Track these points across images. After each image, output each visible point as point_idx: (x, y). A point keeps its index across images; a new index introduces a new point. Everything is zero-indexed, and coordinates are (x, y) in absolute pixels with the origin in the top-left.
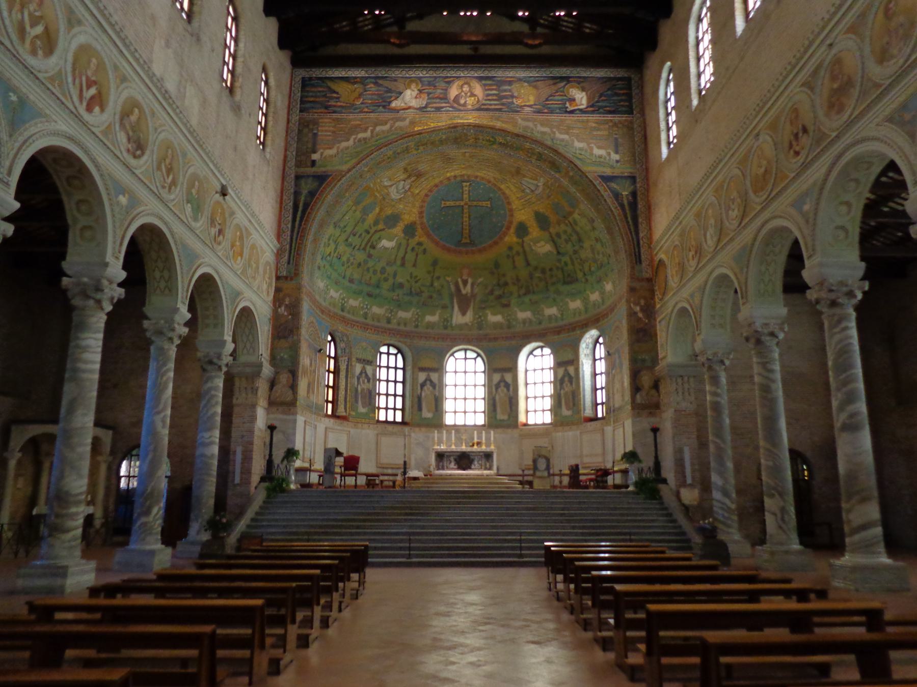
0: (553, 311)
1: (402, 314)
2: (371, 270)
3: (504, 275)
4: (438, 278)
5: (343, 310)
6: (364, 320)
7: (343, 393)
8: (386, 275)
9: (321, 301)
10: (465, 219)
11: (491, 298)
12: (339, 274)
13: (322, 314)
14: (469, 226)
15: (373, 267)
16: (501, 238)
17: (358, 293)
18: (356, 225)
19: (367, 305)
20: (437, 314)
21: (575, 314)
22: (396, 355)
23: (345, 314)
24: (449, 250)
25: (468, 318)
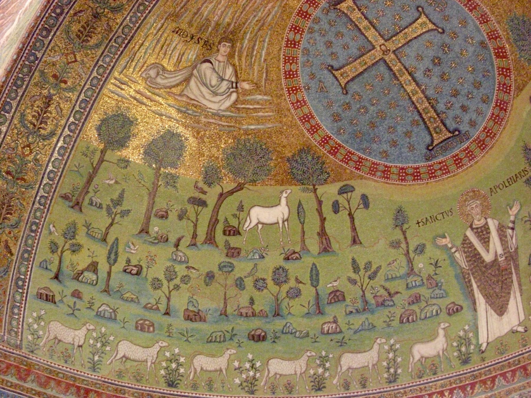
2: (249, 282)
4: (421, 249)
5: (171, 384)
8: (292, 283)
10: (409, 89)
12: (145, 307)
14: (428, 99)
15: (249, 275)
18: (153, 194)
20: (441, 332)
24: (416, 176)
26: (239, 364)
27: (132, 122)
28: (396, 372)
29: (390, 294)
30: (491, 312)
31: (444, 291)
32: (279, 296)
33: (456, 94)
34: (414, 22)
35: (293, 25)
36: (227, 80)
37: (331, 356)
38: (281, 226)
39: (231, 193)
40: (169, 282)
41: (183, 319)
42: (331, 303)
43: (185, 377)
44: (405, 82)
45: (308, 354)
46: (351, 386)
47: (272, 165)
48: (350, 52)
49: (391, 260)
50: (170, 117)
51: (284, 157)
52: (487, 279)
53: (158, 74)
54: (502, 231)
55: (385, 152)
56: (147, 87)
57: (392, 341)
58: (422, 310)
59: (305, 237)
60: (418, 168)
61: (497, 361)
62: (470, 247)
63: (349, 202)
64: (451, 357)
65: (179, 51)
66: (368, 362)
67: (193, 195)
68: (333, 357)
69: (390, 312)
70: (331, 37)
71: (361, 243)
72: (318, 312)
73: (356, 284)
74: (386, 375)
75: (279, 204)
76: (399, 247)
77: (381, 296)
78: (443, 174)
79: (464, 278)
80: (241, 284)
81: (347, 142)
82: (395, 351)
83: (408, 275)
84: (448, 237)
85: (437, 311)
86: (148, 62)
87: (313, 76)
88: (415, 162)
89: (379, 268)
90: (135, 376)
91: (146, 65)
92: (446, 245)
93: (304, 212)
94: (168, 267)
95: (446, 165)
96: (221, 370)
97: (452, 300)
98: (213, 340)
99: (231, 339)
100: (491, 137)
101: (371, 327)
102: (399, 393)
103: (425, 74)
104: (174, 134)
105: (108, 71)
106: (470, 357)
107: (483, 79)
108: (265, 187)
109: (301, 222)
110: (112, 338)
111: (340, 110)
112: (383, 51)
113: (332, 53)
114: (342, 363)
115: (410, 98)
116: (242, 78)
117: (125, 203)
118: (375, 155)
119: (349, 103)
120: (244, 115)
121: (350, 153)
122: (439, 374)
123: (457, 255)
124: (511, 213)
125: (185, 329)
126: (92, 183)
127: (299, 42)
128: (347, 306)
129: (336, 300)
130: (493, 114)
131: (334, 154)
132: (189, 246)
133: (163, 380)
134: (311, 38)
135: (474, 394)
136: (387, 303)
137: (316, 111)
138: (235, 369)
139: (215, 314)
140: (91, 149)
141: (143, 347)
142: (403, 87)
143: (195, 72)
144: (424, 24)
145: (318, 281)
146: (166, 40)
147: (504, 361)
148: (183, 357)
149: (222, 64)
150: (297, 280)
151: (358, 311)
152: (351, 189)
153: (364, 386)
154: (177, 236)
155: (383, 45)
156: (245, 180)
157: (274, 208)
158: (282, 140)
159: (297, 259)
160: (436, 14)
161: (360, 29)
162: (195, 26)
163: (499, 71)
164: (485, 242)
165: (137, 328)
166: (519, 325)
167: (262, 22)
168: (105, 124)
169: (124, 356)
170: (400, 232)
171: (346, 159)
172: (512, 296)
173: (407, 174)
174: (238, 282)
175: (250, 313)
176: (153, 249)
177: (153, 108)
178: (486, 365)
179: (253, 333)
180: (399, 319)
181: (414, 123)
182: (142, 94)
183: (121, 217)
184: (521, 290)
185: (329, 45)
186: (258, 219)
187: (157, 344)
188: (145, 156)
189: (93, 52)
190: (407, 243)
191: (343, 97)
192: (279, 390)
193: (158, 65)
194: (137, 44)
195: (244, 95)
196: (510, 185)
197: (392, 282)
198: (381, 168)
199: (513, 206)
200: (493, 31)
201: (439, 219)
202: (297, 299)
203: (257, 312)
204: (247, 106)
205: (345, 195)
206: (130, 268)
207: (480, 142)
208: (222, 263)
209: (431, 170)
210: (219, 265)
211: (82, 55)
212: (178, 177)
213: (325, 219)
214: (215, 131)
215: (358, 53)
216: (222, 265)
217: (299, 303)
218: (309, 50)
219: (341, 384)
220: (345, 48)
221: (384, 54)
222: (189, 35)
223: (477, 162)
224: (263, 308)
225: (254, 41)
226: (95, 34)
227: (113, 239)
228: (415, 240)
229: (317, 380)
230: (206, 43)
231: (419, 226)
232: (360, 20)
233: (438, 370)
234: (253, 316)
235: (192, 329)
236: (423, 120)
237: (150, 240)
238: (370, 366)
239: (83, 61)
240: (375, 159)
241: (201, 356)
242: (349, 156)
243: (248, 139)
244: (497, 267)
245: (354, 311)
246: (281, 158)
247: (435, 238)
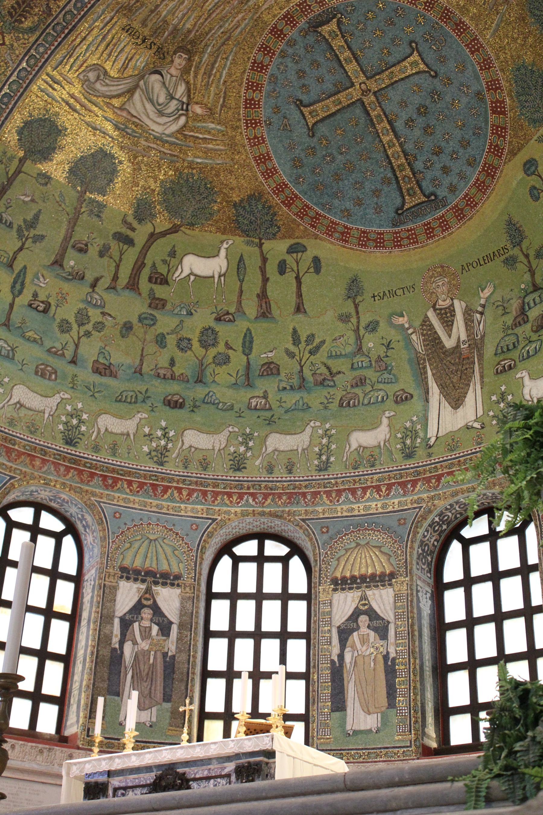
2: (171, 340)
4: (373, 327)
5: (69, 442)
7: (80, 669)
8: (221, 348)
10: (385, 139)
11: (526, 330)
12: (49, 351)
14: (406, 154)
15: (173, 332)
16: (497, 151)
18: (73, 222)
20: (385, 421)
22: (284, 560)
23: (80, 451)
26: (150, 430)
27: (60, 131)
28: (328, 459)
29: (331, 374)
31: (394, 375)
33: (438, 151)
34: (404, 60)
35: (263, 44)
36: (178, 100)
37: (256, 434)
38: (216, 280)
39: (164, 234)
40: (79, 327)
41: (90, 370)
42: (262, 375)
43: (87, 436)
44: (382, 131)
45: (230, 429)
46: (276, 470)
47: (215, 208)
48: (324, 87)
49: (337, 335)
50: (104, 133)
51: (230, 201)
52: (445, 367)
53: (98, 78)
54: (469, 315)
55: (348, 210)
56: (83, 91)
57: (328, 426)
58: (365, 395)
60: (383, 234)
61: (445, 458)
62: (429, 330)
63: (298, 263)
64: (393, 449)
65: (126, 55)
66: (298, 446)
67: (119, 230)
68: (259, 435)
69: (329, 393)
70: (305, 65)
71: (306, 312)
72: (246, 383)
73: (294, 357)
74: (316, 462)
75: (218, 255)
77: (321, 374)
78: (410, 243)
80: (162, 340)
81: (306, 194)
82: (329, 437)
83: (354, 354)
84: (406, 316)
85: (383, 398)
86: (89, 62)
87: (277, 109)
88: (380, 226)
89: (323, 342)
90: (28, 427)
91: (85, 65)
92: (403, 325)
93: (245, 269)
94: (80, 309)
95: (415, 234)
96: (128, 435)
97: (402, 388)
98: (123, 399)
99: (144, 401)
100: (471, 207)
101: (305, 407)
102: (329, 483)
103: (406, 124)
104: (106, 154)
105: (40, 64)
106: (415, 451)
107: (473, 137)
108: (204, 233)
109: (239, 280)
110: (6, 380)
111: (302, 155)
112: (362, 90)
113: (304, 85)
114: (267, 443)
115: (385, 151)
116: (194, 100)
117: (39, 226)
118: (335, 213)
119: (314, 147)
120: (192, 144)
121: (307, 206)
122: (378, 467)
123: (414, 337)
124: (482, 295)
125: (92, 383)
126: (5, 196)
127: (267, 66)
128: (281, 381)
129: (269, 373)
130: (478, 180)
131: (289, 206)
132: (107, 288)
133: (61, 435)
134: (282, 63)
135: (416, 491)
137: (275, 152)
138: (145, 436)
139: (128, 371)
140: (9, 155)
141: (42, 395)
142: (379, 136)
143: (142, 83)
144: (414, 64)
145: (251, 349)
146: (113, 38)
147: (454, 459)
148: (86, 413)
149: (174, 78)
150: (227, 344)
152: (302, 250)
153: (290, 472)
154: (96, 275)
155: (364, 83)
156: (182, 221)
157: (211, 259)
158: (231, 181)
159: (230, 321)
160: (431, 53)
161: (340, 61)
162: (149, 27)
163: (492, 130)
164: (447, 326)
165: (36, 373)
166: (475, 421)
167: (228, 35)
168: (28, 128)
169: (18, 402)
171: (302, 213)
173: (369, 240)
174: (159, 339)
175: (169, 375)
176: (66, 287)
177: (87, 119)
178: (433, 461)
179: (169, 398)
180: (338, 402)
181: (386, 181)
182: (76, 100)
183: (33, 242)
184: (482, 382)
185: (301, 74)
186: (191, 269)
187: (58, 395)
188: (70, 175)
189: (26, 37)
190: (358, 318)
191: (308, 139)
192: (192, 464)
193: (100, 68)
194: (79, 36)
195: (194, 120)
196: (485, 263)
197: (336, 361)
198: (340, 229)
199: (486, 287)
200: (495, 81)
201: (398, 294)
202: (224, 366)
203: (177, 374)
204: (197, 135)
205: (294, 255)
206: (37, 303)
207: (457, 211)
208: (143, 313)
209: (397, 238)
210: (140, 316)
211: (12, 38)
212: (105, 206)
213: (268, 279)
214: (155, 158)
215: (334, 89)
216: (143, 316)
217: (226, 372)
218: (277, 78)
219: (264, 467)
220: (319, 81)
221: (362, 94)
222: (141, 37)
223: (451, 234)
224: (184, 371)
225: (215, 55)
226: (31, 14)
227: (21, 266)
228: (368, 316)
229: (237, 459)
230: (159, 50)
231: (375, 300)
232: (342, 50)
233: (377, 462)
234: (172, 379)
235: (101, 384)
236: (397, 178)
237: (64, 275)
238: (300, 451)
239: (12, 45)
240: (335, 217)
241: (107, 415)
242: (305, 210)
243: (192, 174)
244: (458, 355)
245: (288, 388)
246: (227, 202)
247: (391, 315)
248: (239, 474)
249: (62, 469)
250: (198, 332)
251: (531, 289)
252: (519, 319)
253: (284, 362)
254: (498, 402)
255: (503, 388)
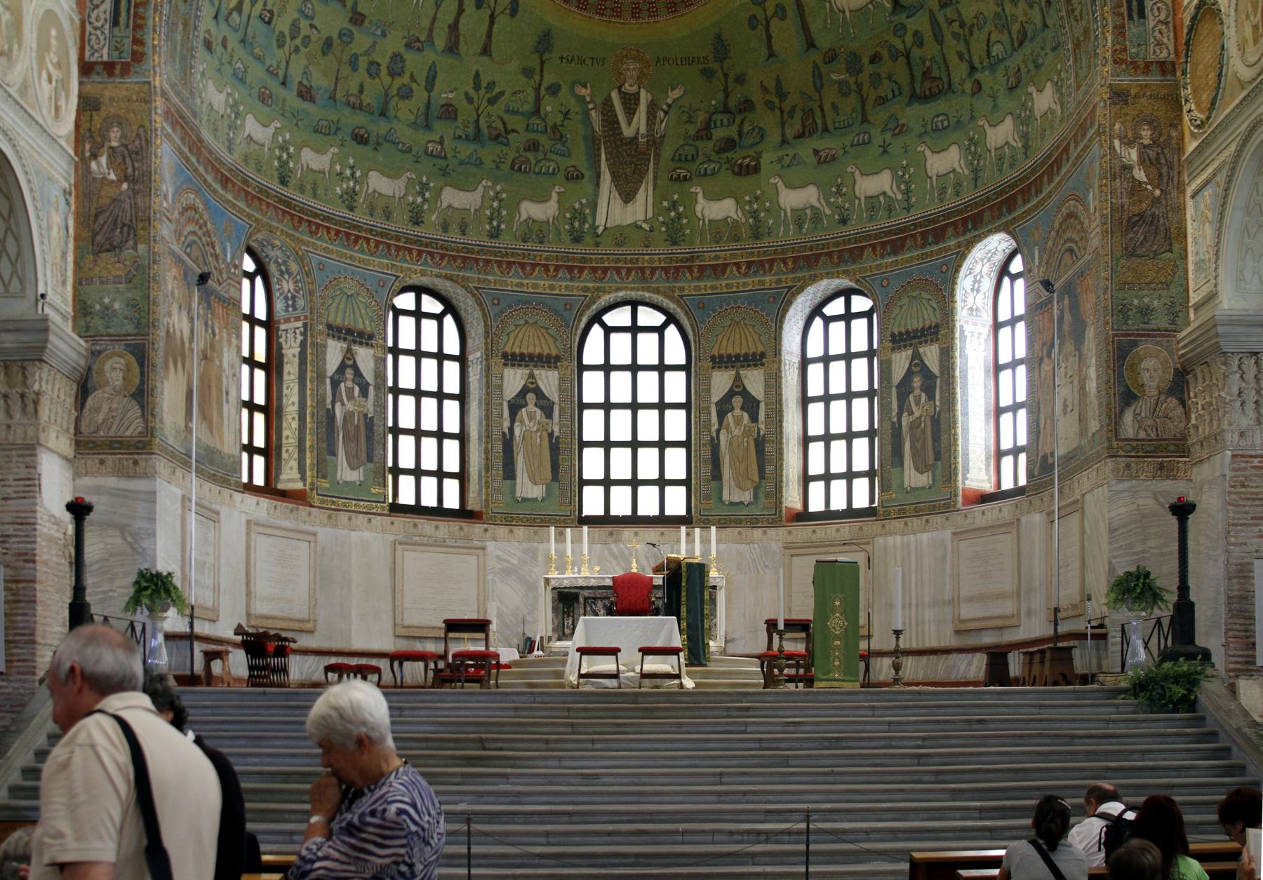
0: (878, 184)
1: (453, 198)
2: (363, 62)
3: (741, 79)
4: (554, 90)
5: (283, 182)
6: (343, 212)
8: (406, 79)
9: (219, 148)
11: (707, 146)
12: (268, 70)
13: (224, 187)
15: (366, 53)
17: (324, 132)
19: (352, 168)
20: (554, 196)
21: (943, 190)
23: (291, 193)
25: (640, 210)
28: (499, 226)
29: (506, 130)
30: (615, 194)
32: (390, 91)
37: (432, 185)
41: (295, 93)
42: (440, 118)
45: (408, 174)
46: (450, 229)
57: (499, 188)
58: (538, 162)
59: (435, 25)
71: (491, 56)
76: (532, 77)
77: (496, 129)
79: (594, 144)
85: (554, 170)
89: (502, 93)
92: (584, 97)
96: (324, 173)
97: (573, 162)
99: (335, 133)
101: (478, 162)
123: (593, 113)
124: (670, 94)
128: (457, 127)
133: (276, 174)
136: (501, 139)
145: (433, 85)
150: (412, 76)
151: (467, 138)
159: (419, 49)
164: (629, 113)
166: (645, 221)
169: (249, 136)
170: (539, 60)
172: (643, 186)
175: (357, 105)
179: (356, 131)
190: (542, 76)
202: (407, 101)
203: (365, 104)
213: (463, 10)
224: (370, 101)
233: (546, 239)
238: (472, 211)
247: (574, 83)
248: (417, 228)
249: (280, 213)
250: (387, 59)
251: (721, 109)
252: (702, 133)
253: (462, 105)
254: (669, 210)
255: (676, 197)
